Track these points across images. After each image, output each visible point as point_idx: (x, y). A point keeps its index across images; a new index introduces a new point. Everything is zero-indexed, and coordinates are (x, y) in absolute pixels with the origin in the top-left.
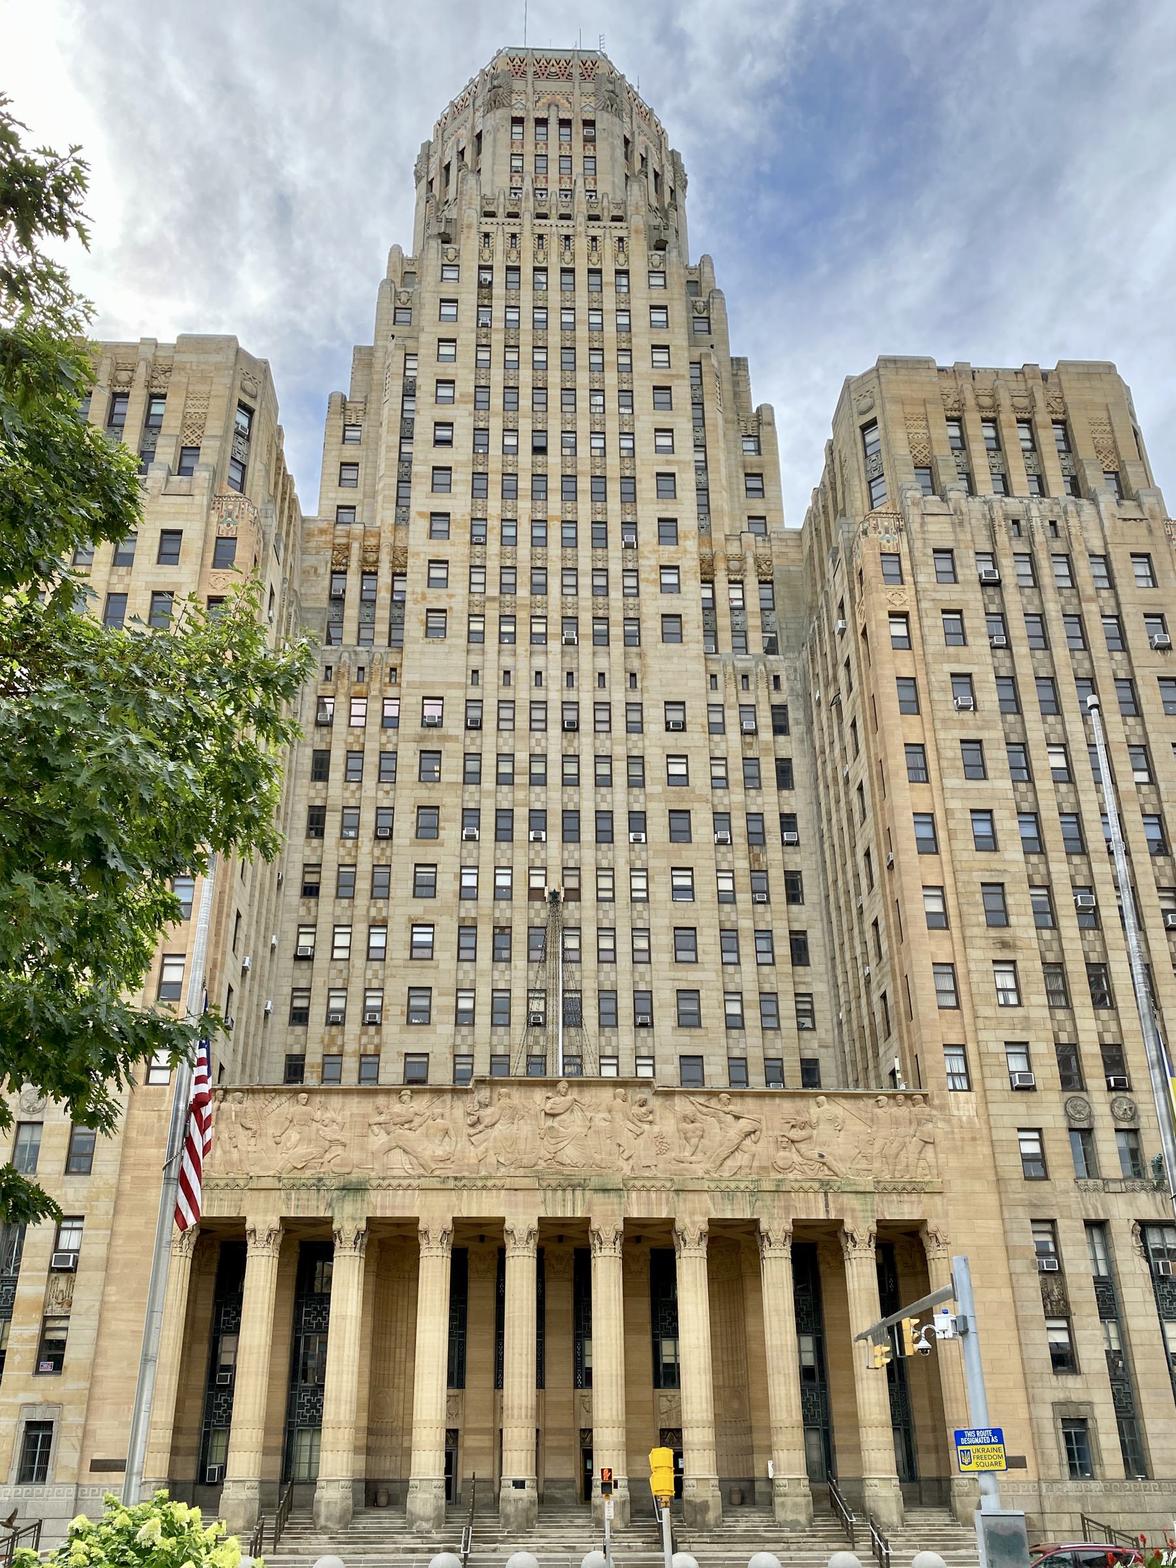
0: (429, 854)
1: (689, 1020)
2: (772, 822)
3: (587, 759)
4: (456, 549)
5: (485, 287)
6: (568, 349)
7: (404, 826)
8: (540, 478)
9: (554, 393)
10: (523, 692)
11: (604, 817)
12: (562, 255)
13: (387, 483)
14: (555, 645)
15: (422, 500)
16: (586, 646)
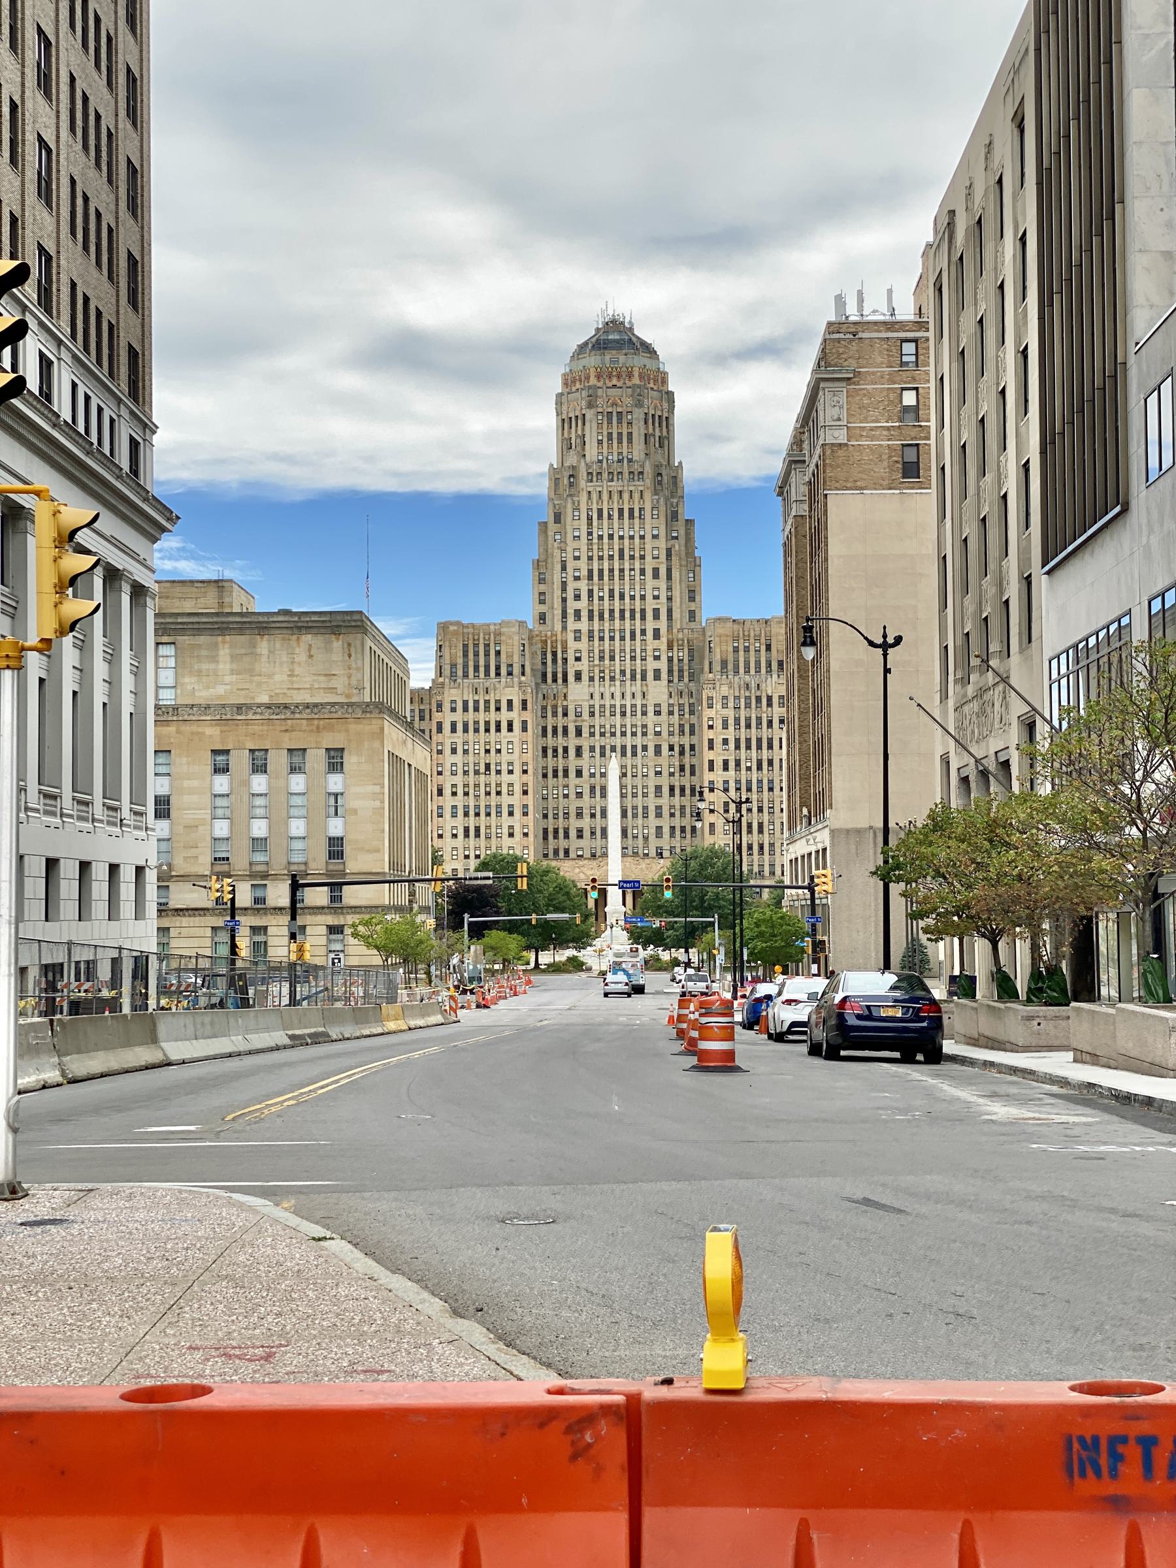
0: (580, 762)
1: (659, 815)
2: (687, 748)
3: (629, 727)
4: (583, 645)
5: (590, 519)
6: (621, 551)
7: (572, 752)
8: (612, 611)
9: (616, 573)
10: (608, 702)
11: (634, 747)
12: (618, 502)
13: (558, 604)
14: (618, 683)
15: (572, 625)
16: (628, 683)
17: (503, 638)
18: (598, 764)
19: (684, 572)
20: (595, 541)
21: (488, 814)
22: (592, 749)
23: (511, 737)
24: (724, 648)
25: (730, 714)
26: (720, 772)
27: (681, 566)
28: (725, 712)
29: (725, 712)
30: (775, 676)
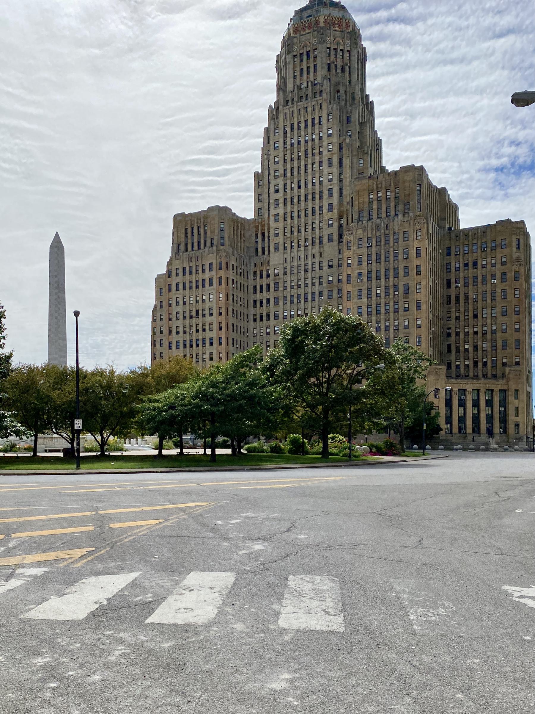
5: (285, 133)
15: (273, 212)
17: (209, 220)
18: (289, 308)
19: (355, 160)
20: (289, 147)
21: (198, 345)
22: (285, 298)
23: (211, 290)
24: (361, 200)
25: (364, 251)
26: (356, 300)
27: (352, 156)
28: (360, 251)
29: (360, 251)
30: (400, 216)
